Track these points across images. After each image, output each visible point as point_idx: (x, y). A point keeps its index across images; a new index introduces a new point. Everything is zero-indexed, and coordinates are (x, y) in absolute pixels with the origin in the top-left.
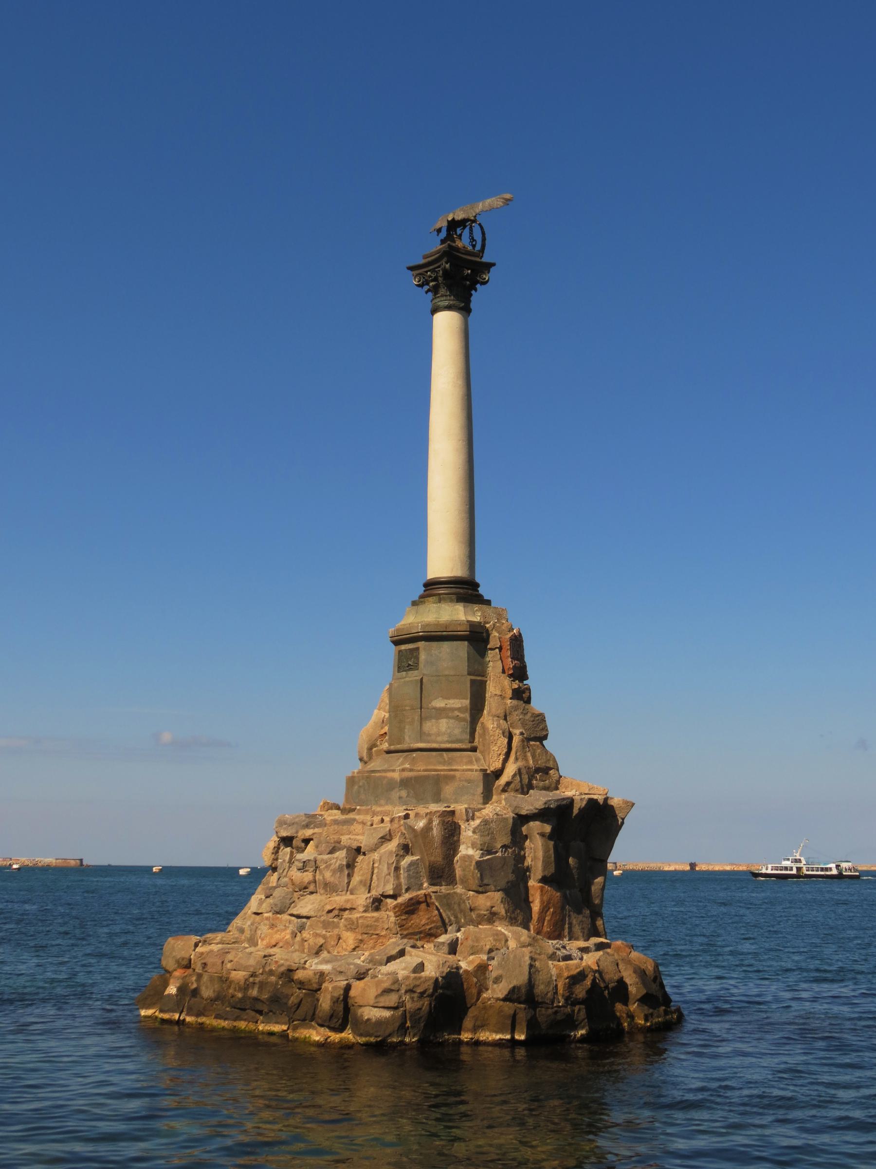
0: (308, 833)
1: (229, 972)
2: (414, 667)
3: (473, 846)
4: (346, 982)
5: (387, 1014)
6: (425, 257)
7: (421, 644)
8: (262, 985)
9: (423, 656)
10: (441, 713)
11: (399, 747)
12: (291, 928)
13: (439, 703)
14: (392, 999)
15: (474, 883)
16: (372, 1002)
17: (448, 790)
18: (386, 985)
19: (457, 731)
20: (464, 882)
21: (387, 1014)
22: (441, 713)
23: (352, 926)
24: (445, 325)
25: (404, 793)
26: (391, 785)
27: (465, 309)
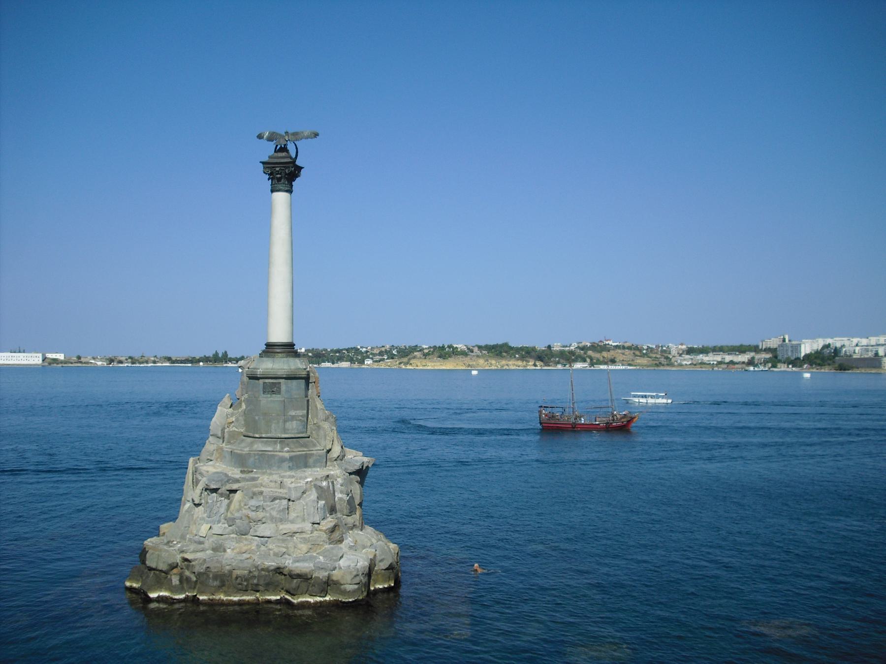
0: (235, 486)
2: (279, 392)
3: (341, 492)
4: (326, 574)
5: (356, 587)
6: (270, 157)
7: (281, 381)
8: (259, 577)
10: (293, 418)
11: (269, 435)
12: (255, 543)
13: (293, 413)
14: (357, 580)
15: (346, 511)
17: (311, 461)
18: (355, 573)
19: (301, 427)
20: (341, 511)
21: (356, 587)
22: (293, 418)
23: (305, 541)
24: (281, 199)
25: (291, 464)
26: (282, 460)
27: (290, 191)
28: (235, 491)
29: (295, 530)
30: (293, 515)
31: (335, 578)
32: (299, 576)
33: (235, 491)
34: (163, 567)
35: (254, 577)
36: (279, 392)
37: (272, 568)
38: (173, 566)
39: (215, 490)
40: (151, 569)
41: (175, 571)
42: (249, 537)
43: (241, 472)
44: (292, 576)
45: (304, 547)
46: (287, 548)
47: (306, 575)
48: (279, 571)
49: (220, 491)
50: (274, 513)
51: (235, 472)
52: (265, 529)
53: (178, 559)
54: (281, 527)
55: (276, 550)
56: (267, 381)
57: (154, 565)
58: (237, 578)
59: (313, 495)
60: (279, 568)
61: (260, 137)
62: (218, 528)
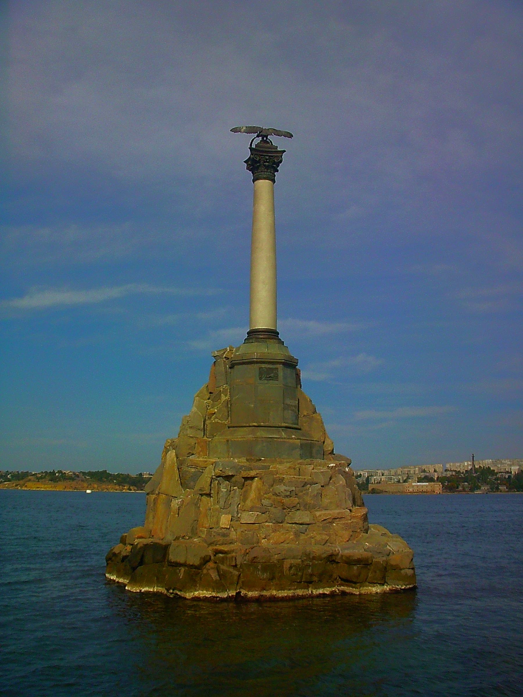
0: (252, 473)
1: (278, 560)
2: (276, 378)
7: (278, 366)
9: (281, 374)
11: (267, 424)
16: (408, 567)
28: (252, 478)
29: (336, 516)
30: (326, 501)
31: (393, 563)
32: (359, 561)
33: (252, 478)
34: (197, 562)
35: (308, 566)
36: (276, 378)
37: (324, 556)
38: (206, 560)
39: (228, 478)
40: (177, 565)
41: (211, 564)
42: (285, 525)
43: (247, 460)
44: (350, 562)
45: (346, 534)
46: (329, 535)
47: (367, 560)
48: (331, 559)
49: (233, 479)
50: (308, 499)
51: (240, 461)
52: (304, 517)
53: (210, 551)
54: (318, 514)
55: (318, 538)
56: (263, 366)
57: (182, 560)
58: (291, 568)
59: (342, 481)
60: (331, 555)
61: (235, 130)
62: (247, 517)
